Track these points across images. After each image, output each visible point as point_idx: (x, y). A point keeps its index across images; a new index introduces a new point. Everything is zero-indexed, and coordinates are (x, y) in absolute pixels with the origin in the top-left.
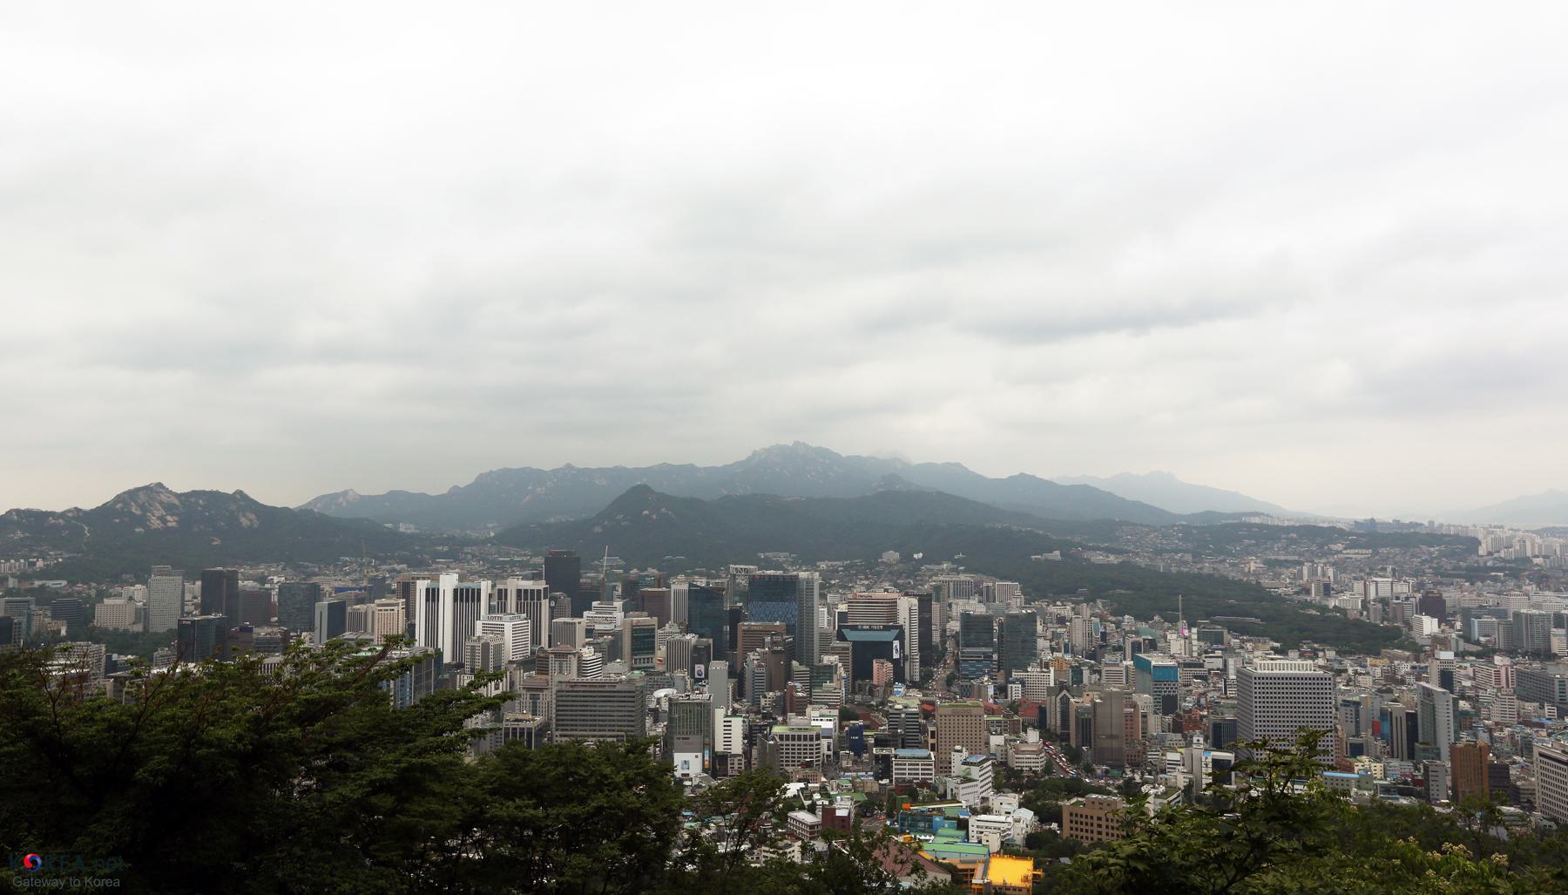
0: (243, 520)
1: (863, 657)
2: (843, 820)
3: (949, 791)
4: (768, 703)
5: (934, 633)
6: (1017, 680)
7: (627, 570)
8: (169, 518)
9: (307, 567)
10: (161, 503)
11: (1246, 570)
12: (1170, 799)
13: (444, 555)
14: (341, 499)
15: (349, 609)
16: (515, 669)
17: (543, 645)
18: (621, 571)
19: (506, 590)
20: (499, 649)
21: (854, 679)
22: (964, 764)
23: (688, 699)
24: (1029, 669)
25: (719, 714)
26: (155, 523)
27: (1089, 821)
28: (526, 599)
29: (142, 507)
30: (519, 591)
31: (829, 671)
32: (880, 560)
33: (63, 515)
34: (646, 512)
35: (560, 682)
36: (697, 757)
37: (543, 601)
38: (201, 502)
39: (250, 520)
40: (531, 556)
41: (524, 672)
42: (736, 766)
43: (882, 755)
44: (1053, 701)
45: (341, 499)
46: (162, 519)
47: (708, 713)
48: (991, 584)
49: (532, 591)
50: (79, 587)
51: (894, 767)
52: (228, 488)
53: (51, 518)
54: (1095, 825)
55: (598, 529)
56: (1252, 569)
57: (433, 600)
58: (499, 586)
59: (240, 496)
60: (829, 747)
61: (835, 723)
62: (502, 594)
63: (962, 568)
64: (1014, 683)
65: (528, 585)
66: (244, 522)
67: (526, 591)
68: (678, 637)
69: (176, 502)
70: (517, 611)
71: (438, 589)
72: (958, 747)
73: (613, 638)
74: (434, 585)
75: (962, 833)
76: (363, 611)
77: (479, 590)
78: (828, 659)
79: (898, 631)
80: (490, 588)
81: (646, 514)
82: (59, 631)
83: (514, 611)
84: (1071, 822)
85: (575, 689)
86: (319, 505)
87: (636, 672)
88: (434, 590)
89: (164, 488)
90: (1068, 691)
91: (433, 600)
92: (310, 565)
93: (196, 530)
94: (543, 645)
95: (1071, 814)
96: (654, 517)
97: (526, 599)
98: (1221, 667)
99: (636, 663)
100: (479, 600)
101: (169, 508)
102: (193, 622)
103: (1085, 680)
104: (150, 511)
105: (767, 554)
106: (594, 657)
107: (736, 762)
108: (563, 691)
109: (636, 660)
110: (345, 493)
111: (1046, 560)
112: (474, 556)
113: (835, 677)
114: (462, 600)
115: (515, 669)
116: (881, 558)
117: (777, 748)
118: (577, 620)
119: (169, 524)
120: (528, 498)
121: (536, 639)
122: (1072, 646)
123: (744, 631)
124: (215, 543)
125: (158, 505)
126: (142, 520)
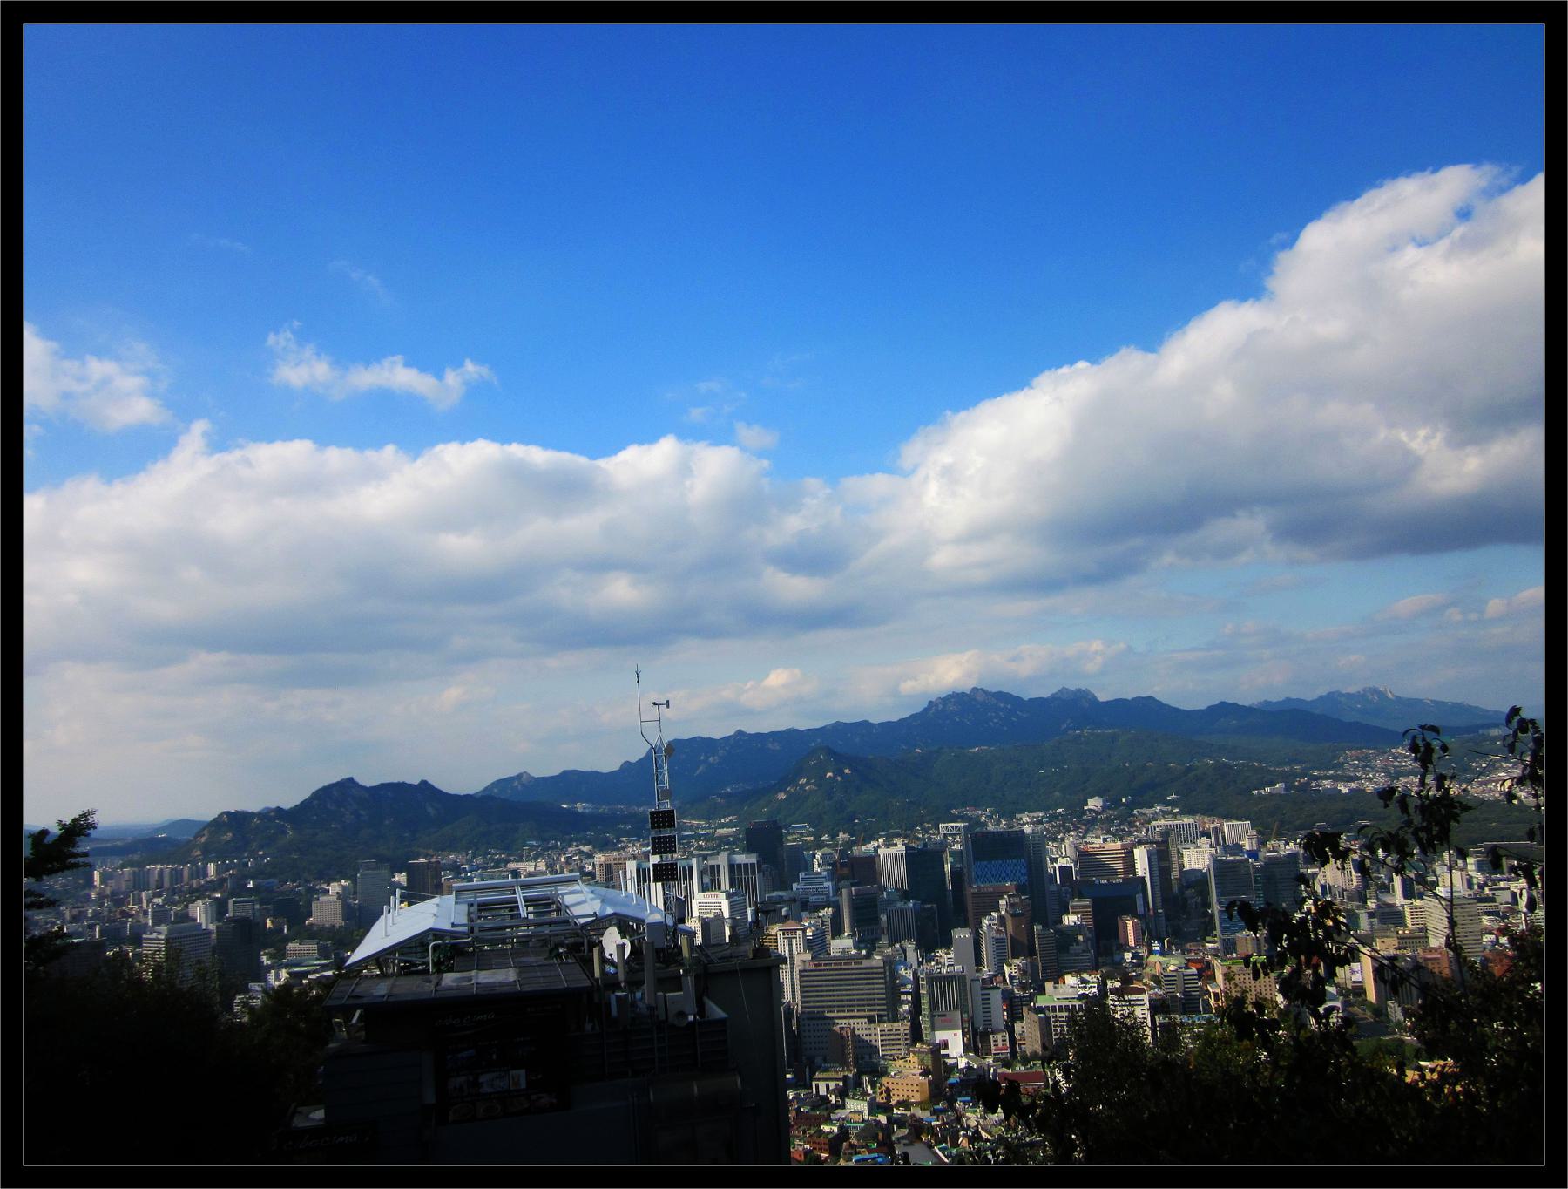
0: (430, 810)
4: (1013, 971)
14: (516, 784)
18: (812, 838)
19: (718, 866)
32: (1086, 808)
34: (829, 775)
36: (956, 1035)
42: (1000, 1044)
45: (516, 784)
49: (746, 865)
65: (741, 859)
67: (739, 865)
68: (899, 904)
81: (830, 776)
83: (728, 888)
85: (819, 968)
100: (691, 878)
107: (999, 1037)
108: (806, 971)
110: (519, 776)
116: (1087, 805)
120: (701, 768)
123: (973, 894)
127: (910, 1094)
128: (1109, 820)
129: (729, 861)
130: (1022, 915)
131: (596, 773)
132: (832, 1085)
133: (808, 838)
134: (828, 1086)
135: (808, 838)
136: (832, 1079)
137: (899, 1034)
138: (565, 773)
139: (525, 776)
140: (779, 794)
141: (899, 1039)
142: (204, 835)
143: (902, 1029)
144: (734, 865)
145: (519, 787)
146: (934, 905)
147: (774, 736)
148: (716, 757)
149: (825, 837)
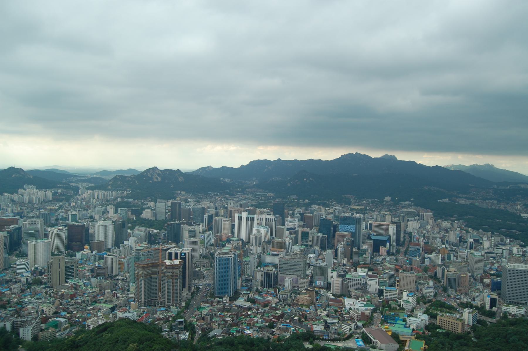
0: (179, 179)
1: (377, 246)
2: (367, 317)
3: (402, 305)
5: (401, 234)
6: (428, 257)
7: (299, 200)
8: (159, 178)
9: (199, 195)
10: (156, 173)
11: (516, 208)
12: (474, 314)
13: (239, 192)
14: (207, 169)
15: (214, 219)
16: (265, 244)
17: (273, 236)
18: (297, 200)
19: (262, 218)
20: (260, 238)
21: (374, 252)
22: (407, 296)
24: (433, 254)
25: (330, 270)
26: (155, 180)
27: (445, 322)
28: (268, 221)
29: (151, 174)
30: (266, 219)
31: (365, 251)
32: (384, 200)
33: (130, 177)
34: (305, 179)
39: (182, 179)
40: (268, 193)
43: (381, 289)
44: (439, 269)
45: (207, 169)
46: (157, 178)
47: (326, 270)
48: (422, 213)
49: (270, 219)
50: (136, 201)
51: (385, 294)
52: (175, 168)
54: (447, 323)
55: (289, 185)
56: (518, 208)
58: (260, 217)
59: (178, 171)
60: (364, 281)
61: (366, 274)
62: (261, 219)
63: (413, 204)
64: (427, 259)
67: (268, 219)
69: (160, 173)
72: (405, 290)
74: (240, 215)
75: (404, 323)
76: (218, 219)
77: (254, 218)
78: (365, 247)
79: (388, 237)
82: (133, 218)
83: (264, 225)
84: (440, 321)
86: (200, 171)
87: (303, 246)
88: (240, 217)
89: (157, 168)
90: (445, 266)
94: (273, 236)
95: (440, 319)
96: (308, 181)
97: (268, 221)
98: (501, 253)
100: (254, 221)
101: (159, 175)
102: (172, 224)
103: (452, 259)
104: (153, 176)
105: (345, 196)
110: (208, 167)
111: (444, 202)
112: (249, 192)
113: (367, 253)
114: (249, 220)
115: (265, 244)
117: (347, 284)
118: (284, 227)
119: (159, 180)
120: (266, 170)
121: (271, 234)
122: (449, 242)
126: (151, 179)
128: (390, 205)
130: (349, 245)
131: (232, 168)
132: (284, 296)
133: (295, 200)
134: (282, 296)
135: (295, 200)
136: (283, 294)
138: (223, 167)
143: (306, 282)
145: (208, 171)
146: (327, 236)
147: (290, 161)
149: (301, 201)
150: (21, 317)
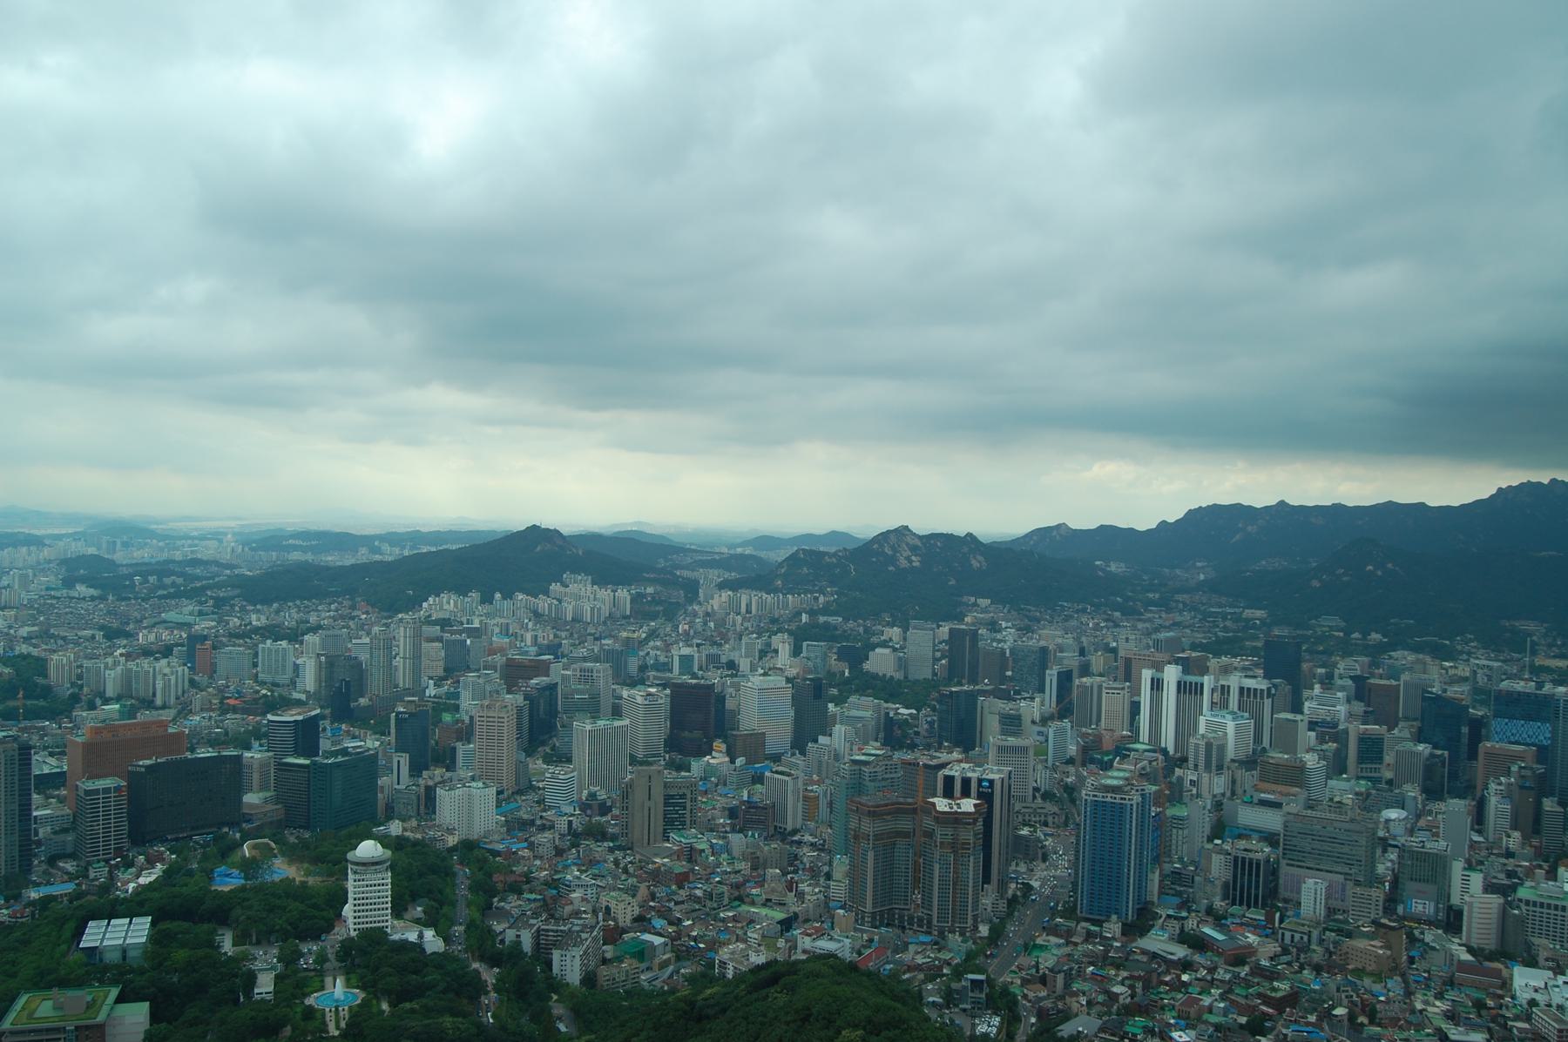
0: (973, 562)
7: (1347, 634)
8: (913, 558)
9: (1030, 611)
10: (907, 544)
14: (1055, 533)
15: (1077, 682)
16: (1237, 768)
17: (1264, 745)
18: (1341, 634)
19: (1229, 687)
20: (1222, 748)
23: (1423, 847)
25: (1457, 867)
26: (903, 563)
28: (1249, 696)
29: (893, 548)
33: (835, 555)
34: (1370, 567)
35: (1289, 813)
37: (1265, 700)
38: (939, 544)
39: (980, 562)
40: (1244, 608)
41: (1246, 771)
45: (1055, 533)
46: (908, 559)
47: (1445, 867)
49: (1255, 690)
50: (851, 624)
52: (960, 530)
53: (827, 557)
55: (1315, 583)
57: (1158, 689)
58: (1223, 683)
59: (970, 537)
62: (1225, 690)
65: (1250, 683)
66: (975, 564)
67: (1249, 689)
69: (919, 544)
70: (1239, 710)
71: (1163, 680)
73: (1339, 746)
74: (1159, 675)
76: (1088, 684)
77: (1202, 685)
80: (1212, 681)
81: (1370, 570)
83: (1236, 709)
87: (1362, 782)
88: (1158, 680)
89: (910, 530)
91: (1158, 689)
92: (1033, 609)
93: (935, 570)
94: (1264, 745)
96: (1379, 573)
97: (1249, 696)
99: (1362, 771)
100: (1202, 693)
101: (914, 549)
102: (952, 692)
105: (1512, 623)
106: (1319, 766)
109: (1362, 768)
110: (1059, 526)
114: (1185, 692)
115: (1237, 768)
117: (1521, 920)
118: (1299, 717)
119: (914, 564)
120: (1238, 537)
121: (1258, 738)
124: (951, 583)
125: (904, 546)
126: (892, 560)
127: (1368, 962)
129: (1240, 683)
130: (1530, 788)
131: (1132, 530)
134: (1293, 937)
136: (1296, 931)
137: (1370, 900)
139: (1063, 527)
140: (1313, 581)
141: (1370, 904)
142: (783, 567)
144: (1243, 688)
145: (1058, 537)
146: (1446, 752)
147: (1318, 509)
148: (1255, 527)
149: (1356, 635)
150: (1087, 929)
